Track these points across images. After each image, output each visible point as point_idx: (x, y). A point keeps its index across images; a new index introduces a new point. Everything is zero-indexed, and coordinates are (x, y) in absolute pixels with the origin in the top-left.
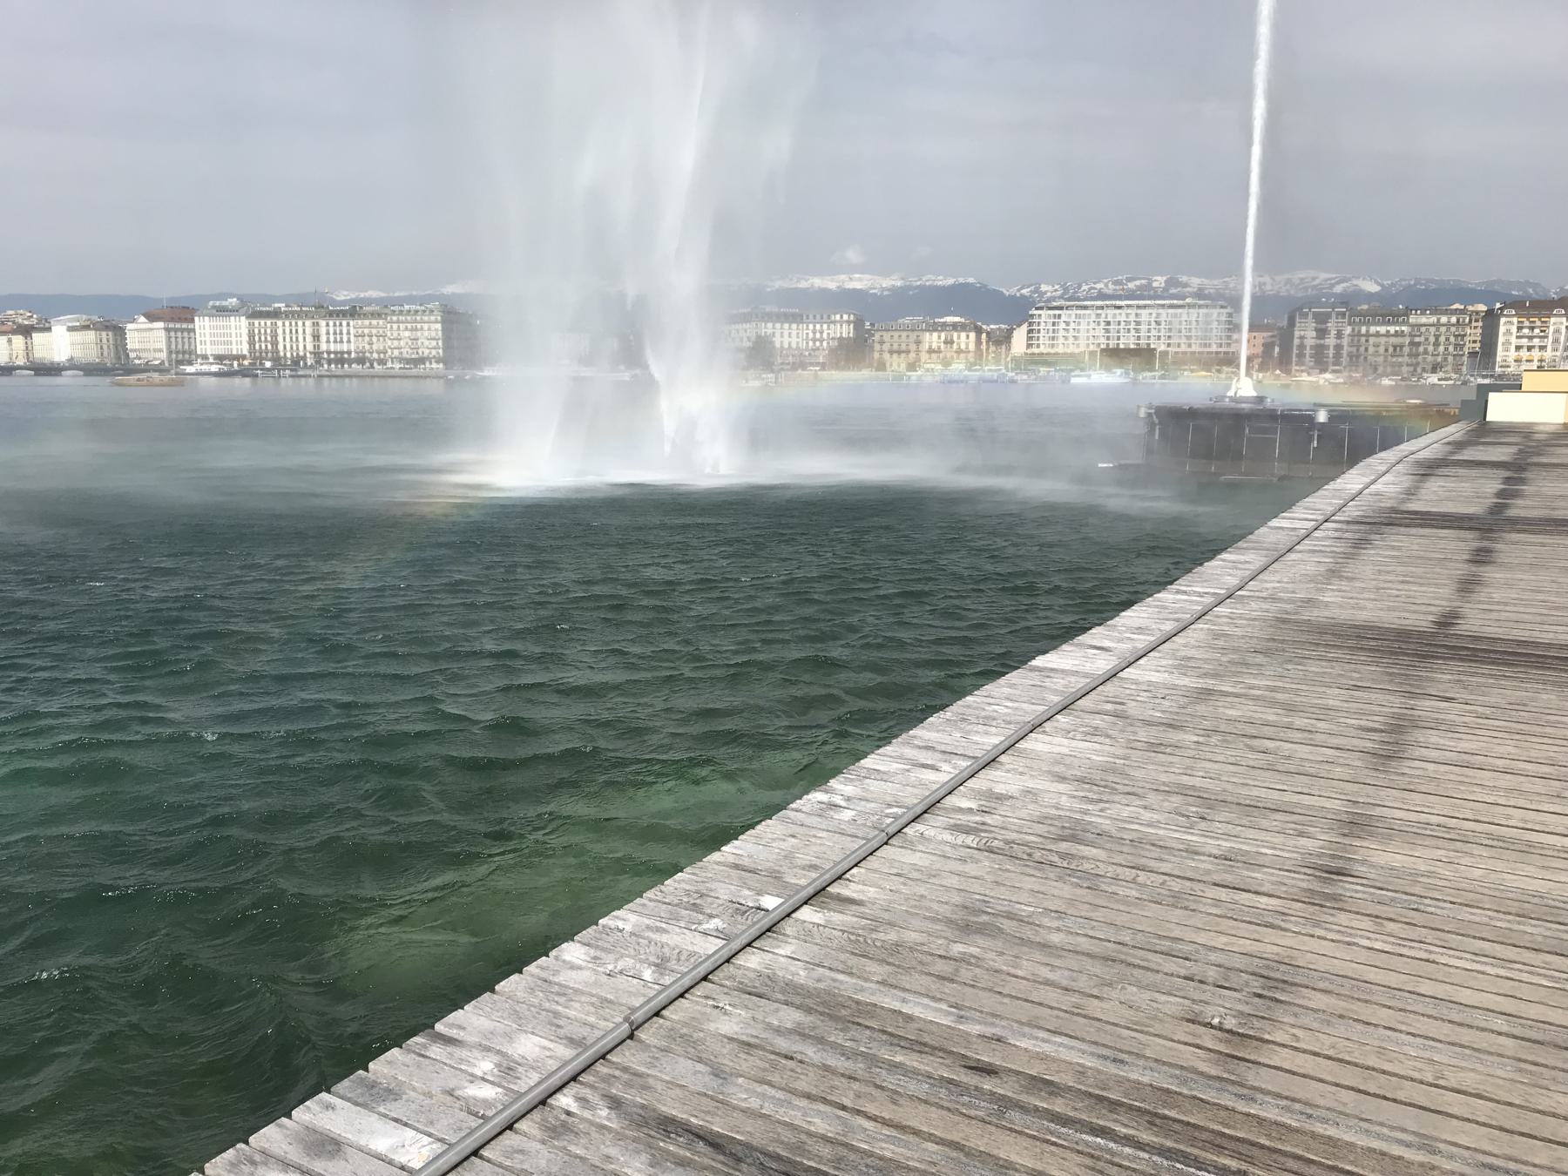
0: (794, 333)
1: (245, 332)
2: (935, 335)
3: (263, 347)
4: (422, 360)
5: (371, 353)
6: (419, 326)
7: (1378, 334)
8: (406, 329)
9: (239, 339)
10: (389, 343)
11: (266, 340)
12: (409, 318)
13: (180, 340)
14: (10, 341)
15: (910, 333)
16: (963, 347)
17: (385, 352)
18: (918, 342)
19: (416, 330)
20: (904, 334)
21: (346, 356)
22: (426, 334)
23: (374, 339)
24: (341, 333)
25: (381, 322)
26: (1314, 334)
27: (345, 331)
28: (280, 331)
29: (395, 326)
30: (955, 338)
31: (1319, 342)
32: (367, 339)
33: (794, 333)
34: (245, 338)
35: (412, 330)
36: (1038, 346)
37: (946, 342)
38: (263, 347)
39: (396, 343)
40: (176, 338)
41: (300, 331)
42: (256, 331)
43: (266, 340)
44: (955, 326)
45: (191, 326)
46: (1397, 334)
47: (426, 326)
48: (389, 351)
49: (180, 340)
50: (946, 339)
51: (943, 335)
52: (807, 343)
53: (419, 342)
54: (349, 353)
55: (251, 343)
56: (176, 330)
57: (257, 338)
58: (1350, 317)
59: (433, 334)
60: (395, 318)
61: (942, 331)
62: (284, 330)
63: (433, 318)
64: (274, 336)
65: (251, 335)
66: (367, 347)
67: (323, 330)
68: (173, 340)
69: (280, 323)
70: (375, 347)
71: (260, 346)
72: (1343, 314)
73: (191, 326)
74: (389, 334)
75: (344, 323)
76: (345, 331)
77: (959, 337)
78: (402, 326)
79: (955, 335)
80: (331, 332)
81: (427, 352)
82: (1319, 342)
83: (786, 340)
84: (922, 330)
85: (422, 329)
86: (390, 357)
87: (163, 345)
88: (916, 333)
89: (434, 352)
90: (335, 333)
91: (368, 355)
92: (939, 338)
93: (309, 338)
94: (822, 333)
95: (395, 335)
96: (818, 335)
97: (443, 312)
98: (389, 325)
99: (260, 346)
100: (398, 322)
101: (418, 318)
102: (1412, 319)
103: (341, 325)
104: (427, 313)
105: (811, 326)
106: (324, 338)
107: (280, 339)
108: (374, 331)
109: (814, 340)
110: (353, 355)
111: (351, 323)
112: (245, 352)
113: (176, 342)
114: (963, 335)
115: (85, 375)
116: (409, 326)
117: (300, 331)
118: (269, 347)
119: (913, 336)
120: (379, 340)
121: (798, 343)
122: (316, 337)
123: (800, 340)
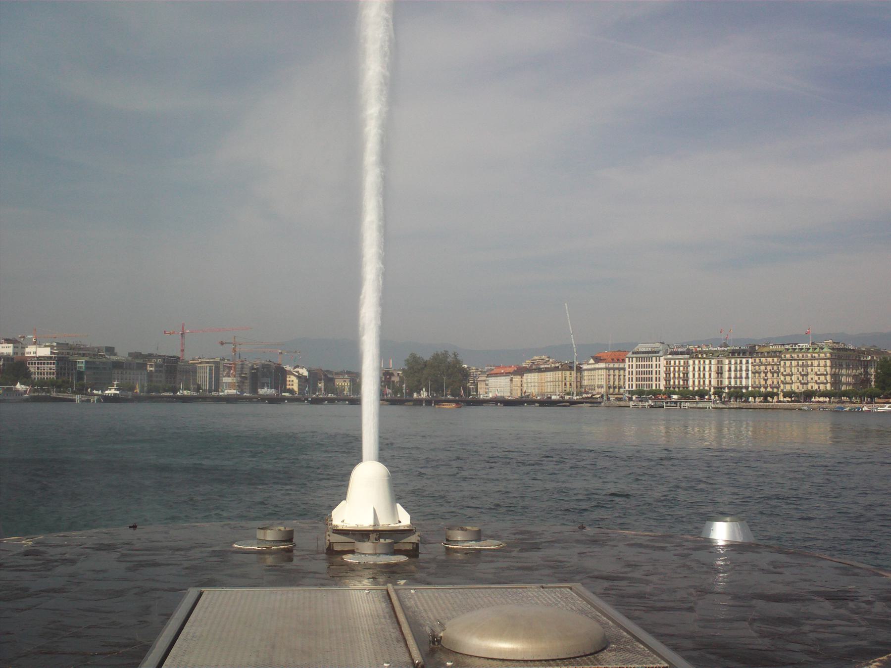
1: (663, 369)
3: (677, 383)
4: (808, 395)
5: (766, 388)
6: (809, 362)
8: (798, 366)
9: (658, 376)
10: (782, 378)
11: (679, 377)
12: (800, 355)
14: (511, 380)
17: (778, 388)
19: (807, 366)
21: (744, 391)
22: (815, 369)
23: (769, 375)
24: (741, 370)
25: (776, 360)
27: (744, 368)
28: (691, 369)
29: (788, 363)
32: (763, 375)
34: (663, 375)
35: (803, 366)
38: (677, 383)
40: (614, 375)
41: (707, 368)
42: (672, 369)
43: (679, 377)
45: (622, 366)
47: (815, 363)
48: (782, 386)
53: (809, 377)
54: (747, 387)
55: (667, 380)
56: (614, 369)
57: (672, 375)
59: (822, 370)
60: (788, 356)
62: (694, 368)
63: (822, 355)
64: (686, 374)
66: (763, 382)
67: (726, 368)
68: (612, 377)
70: (769, 382)
71: (674, 382)
73: (622, 366)
74: (782, 370)
75: (744, 361)
76: (744, 368)
78: (794, 363)
80: (733, 368)
81: (816, 387)
85: (812, 365)
86: (782, 391)
87: (604, 383)
89: (822, 387)
90: (736, 370)
91: (762, 389)
93: (713, 375)
95: (788, 370)
97: (833, 349)
98: (782, 363)
99: (674, 382)
100: (793, 359)
101: (809, 355)
103: (741, 363)
104: (817, 350)
106: (726, 374)
107: (691, 375)
108: (769, 367)
110: (750, 389)
111: (750, 361)
112: (662, 388)
113: (614, 379)
115: (540, 406)
116: (800, 363)
117: (707, 368)
118: (681, 383)
120: (773, 376)
122: (720, 372)
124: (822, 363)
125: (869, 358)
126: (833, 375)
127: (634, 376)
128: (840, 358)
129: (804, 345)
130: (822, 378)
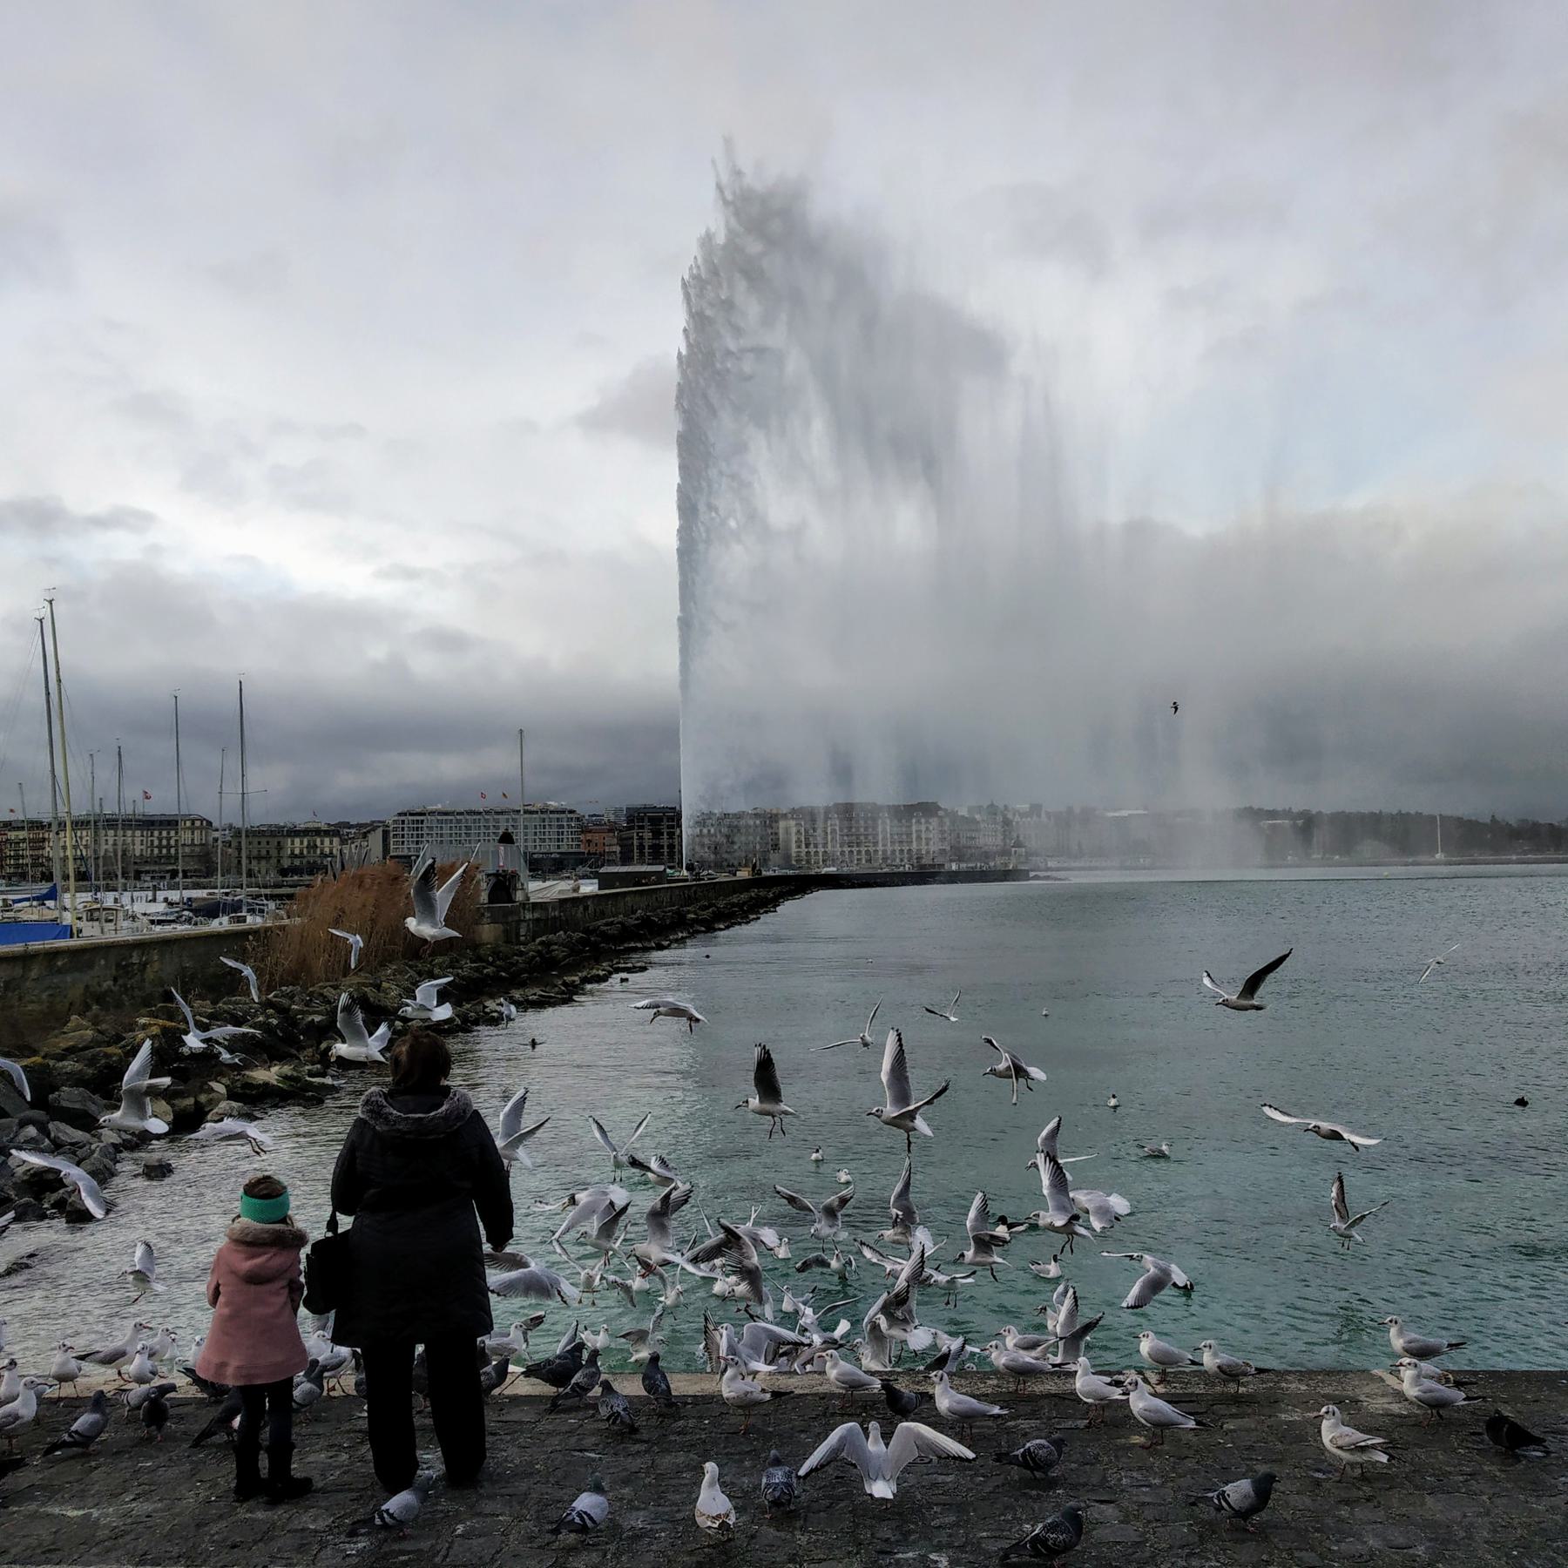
0: (138, 840)
2: (297, 841)
15: (270, 839)
16: (327, 850)
18: (280, 847)
20: (264, 841)
30: (318, 843)
33: (138, 840)
50: (309, 844)
52: (152, 851)
61: (305, 836)
77: (322, 843)
84: (283, 835)
88: (276, 840)
92: (302, 843)
94: (169, 839)
96: (164, 842)
105: (156, 833)
109: (160, 847)
114: (327, 841)
119: (274, 842)
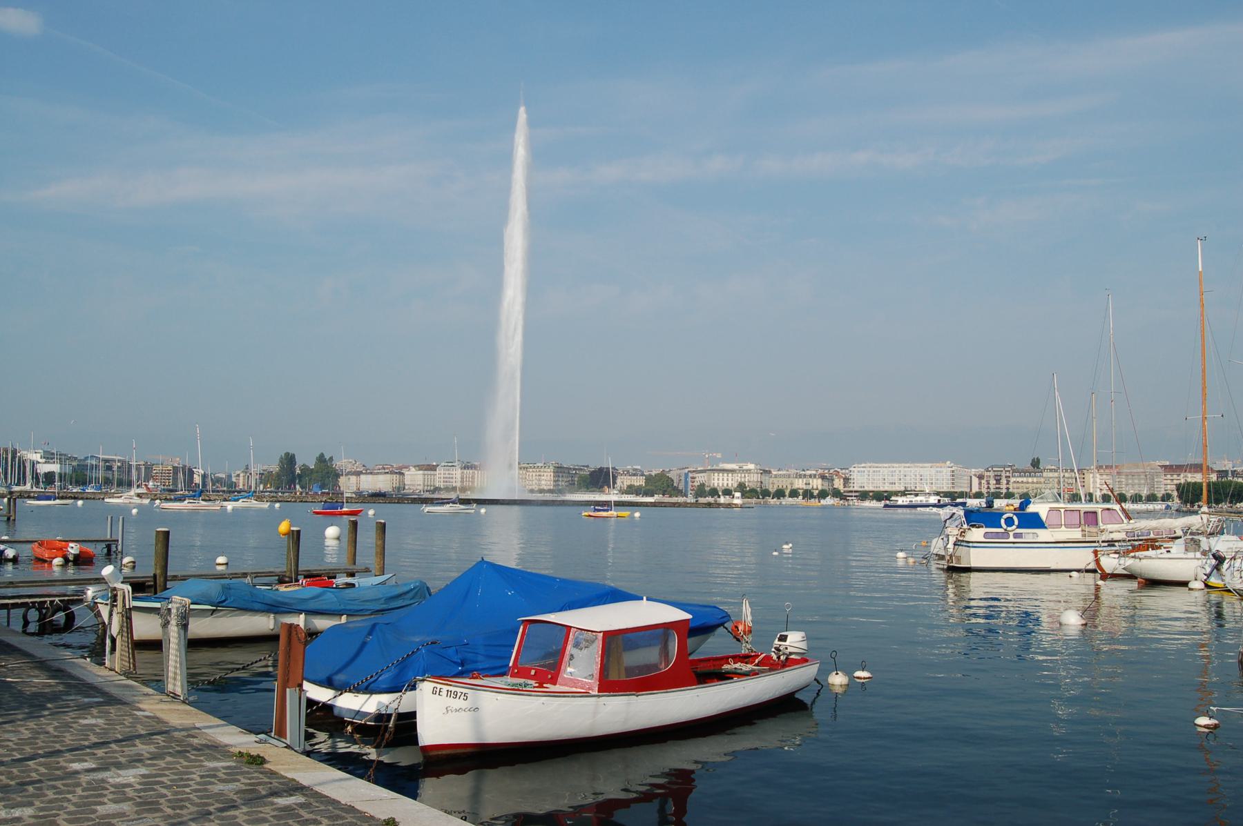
2: (800, 480)
6: (542, 474)
7: (1028, 483)
13: (429, 480)
25: (524, 472)
26: (995, 482)
28: (476, 476)
29: (531, 474)
30: (811, 482)
31: (997, 486)
36: (854, 487)
37: (806, 484)
39: (531, 482)
44: (810, 476)
46: (1037, 483)
47: (545, 474)
49: (429, 480)
51: (805, 480)
55: (462, 481)
58: (1013, 473)
60: (531, 470)
63: (549, 470)
65: (462, 478)
69: (476, 472)
72: (1009, 471)
77: (813, 482)
78: (534, 474)
79: (811, 480)
82: (997, 486)
83: (725, 482)
102: (1045, 474)
107: (476, 480)
114: (815, 480)
116: (538, 474)
121: (732, 484)
123: (733, 482)
124: (549, 474)
125: (574, 472)
126: (554, 481)
127: (442, 480)
128: (557, 472)
129: (540, 465)
130: (549, 482)
